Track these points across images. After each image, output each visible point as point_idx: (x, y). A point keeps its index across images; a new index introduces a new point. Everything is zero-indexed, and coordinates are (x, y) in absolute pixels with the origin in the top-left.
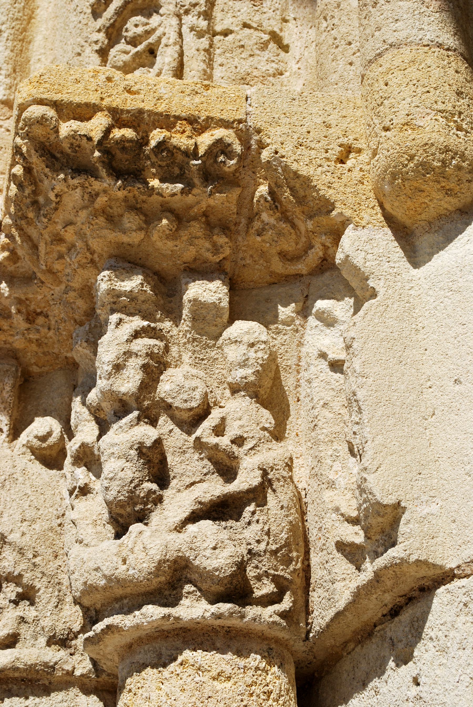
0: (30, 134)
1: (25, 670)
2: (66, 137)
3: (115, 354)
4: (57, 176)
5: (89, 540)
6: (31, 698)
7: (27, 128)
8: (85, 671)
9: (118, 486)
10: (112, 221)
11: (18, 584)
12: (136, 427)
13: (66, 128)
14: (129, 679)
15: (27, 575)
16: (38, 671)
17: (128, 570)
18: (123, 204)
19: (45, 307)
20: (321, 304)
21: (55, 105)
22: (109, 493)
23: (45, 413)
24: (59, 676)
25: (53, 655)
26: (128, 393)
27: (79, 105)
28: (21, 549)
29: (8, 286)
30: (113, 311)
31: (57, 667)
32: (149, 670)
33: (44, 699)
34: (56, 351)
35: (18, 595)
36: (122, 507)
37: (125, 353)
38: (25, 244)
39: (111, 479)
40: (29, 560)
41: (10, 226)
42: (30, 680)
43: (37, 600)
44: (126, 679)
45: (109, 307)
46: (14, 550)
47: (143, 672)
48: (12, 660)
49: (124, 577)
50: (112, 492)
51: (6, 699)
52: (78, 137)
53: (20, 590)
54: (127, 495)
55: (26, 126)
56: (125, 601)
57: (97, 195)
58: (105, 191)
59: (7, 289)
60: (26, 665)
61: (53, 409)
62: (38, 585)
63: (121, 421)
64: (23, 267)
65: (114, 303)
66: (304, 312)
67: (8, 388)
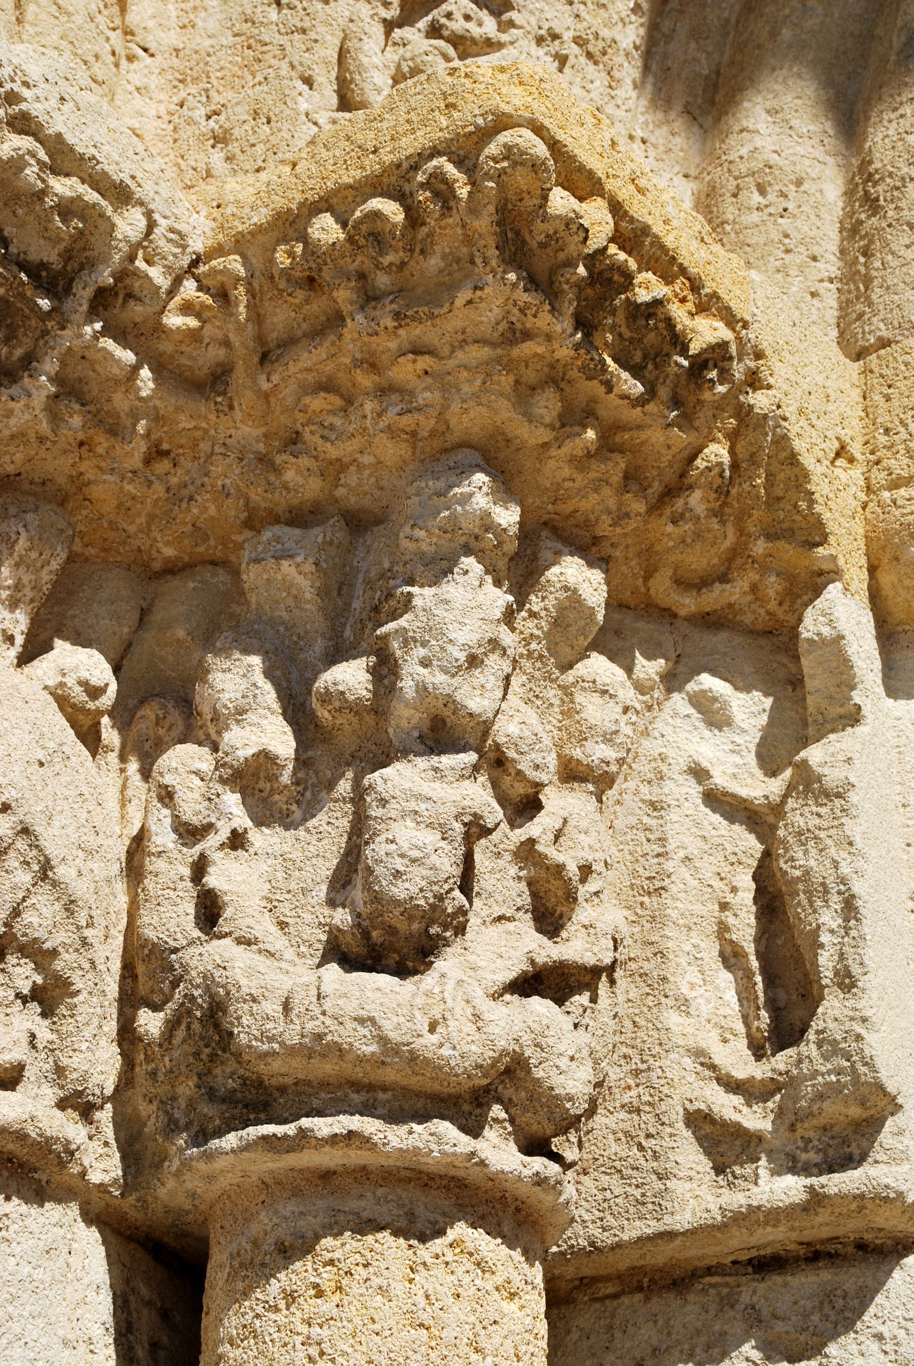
0: (503, 177)
1: (35, 1143)
2: (559, 217)
3: (478, 636)
4: (505, 272)
5: (278, 947)
6: (15, 1200)
7: (505, 164)
8: (107, 1179)
9: (423, 878)
10: (524, 394)
11: (38, 968)
12: (467, 782)
13: (561, 201)
14: (330, 1239)
15: (66, 956)
16: (51, 1152)
17: (441, 1045)
18: (546, 370)
19: (182, 447)
20: (707, 681)
21: (554, 145)
22: (399, 882)
23: (81, 640)
24: (72, 1175)
25: (68, 1128)
26: (480, 715)
27: (581, 168)
28: (72, 902)
29: (155, 380)
30: (468, 551)
31: (77, 1155)
32: (385, 1236)
33: (34, 1210)
34: (132, 529)
35: (35, 988)
36: (411, 918)
37: (490, 641)
38: (250, 326)
39: (413, 861)
40: (79, 928)
41: (238, 279)
42: (21, 1165)
44: (317, 1238)
45: (464, 538)
47: (370, 1238)
48: (24, 1117)
49: (430, 1055)
50: (407, 885)
52: (574, 227)
53: (39, 980)
54: (432, 900)
55: (506, 158)
56: (381, 1096)
57: (527, 335)
58: (549, 338)
59: (151, 385)
60: (41, 1135)
61: (94, 636)
62: (79, 984)
63: (436, 758)
64: (190, 357)
65: (476, 538)
66: (672, 681)
67: (55, 565)
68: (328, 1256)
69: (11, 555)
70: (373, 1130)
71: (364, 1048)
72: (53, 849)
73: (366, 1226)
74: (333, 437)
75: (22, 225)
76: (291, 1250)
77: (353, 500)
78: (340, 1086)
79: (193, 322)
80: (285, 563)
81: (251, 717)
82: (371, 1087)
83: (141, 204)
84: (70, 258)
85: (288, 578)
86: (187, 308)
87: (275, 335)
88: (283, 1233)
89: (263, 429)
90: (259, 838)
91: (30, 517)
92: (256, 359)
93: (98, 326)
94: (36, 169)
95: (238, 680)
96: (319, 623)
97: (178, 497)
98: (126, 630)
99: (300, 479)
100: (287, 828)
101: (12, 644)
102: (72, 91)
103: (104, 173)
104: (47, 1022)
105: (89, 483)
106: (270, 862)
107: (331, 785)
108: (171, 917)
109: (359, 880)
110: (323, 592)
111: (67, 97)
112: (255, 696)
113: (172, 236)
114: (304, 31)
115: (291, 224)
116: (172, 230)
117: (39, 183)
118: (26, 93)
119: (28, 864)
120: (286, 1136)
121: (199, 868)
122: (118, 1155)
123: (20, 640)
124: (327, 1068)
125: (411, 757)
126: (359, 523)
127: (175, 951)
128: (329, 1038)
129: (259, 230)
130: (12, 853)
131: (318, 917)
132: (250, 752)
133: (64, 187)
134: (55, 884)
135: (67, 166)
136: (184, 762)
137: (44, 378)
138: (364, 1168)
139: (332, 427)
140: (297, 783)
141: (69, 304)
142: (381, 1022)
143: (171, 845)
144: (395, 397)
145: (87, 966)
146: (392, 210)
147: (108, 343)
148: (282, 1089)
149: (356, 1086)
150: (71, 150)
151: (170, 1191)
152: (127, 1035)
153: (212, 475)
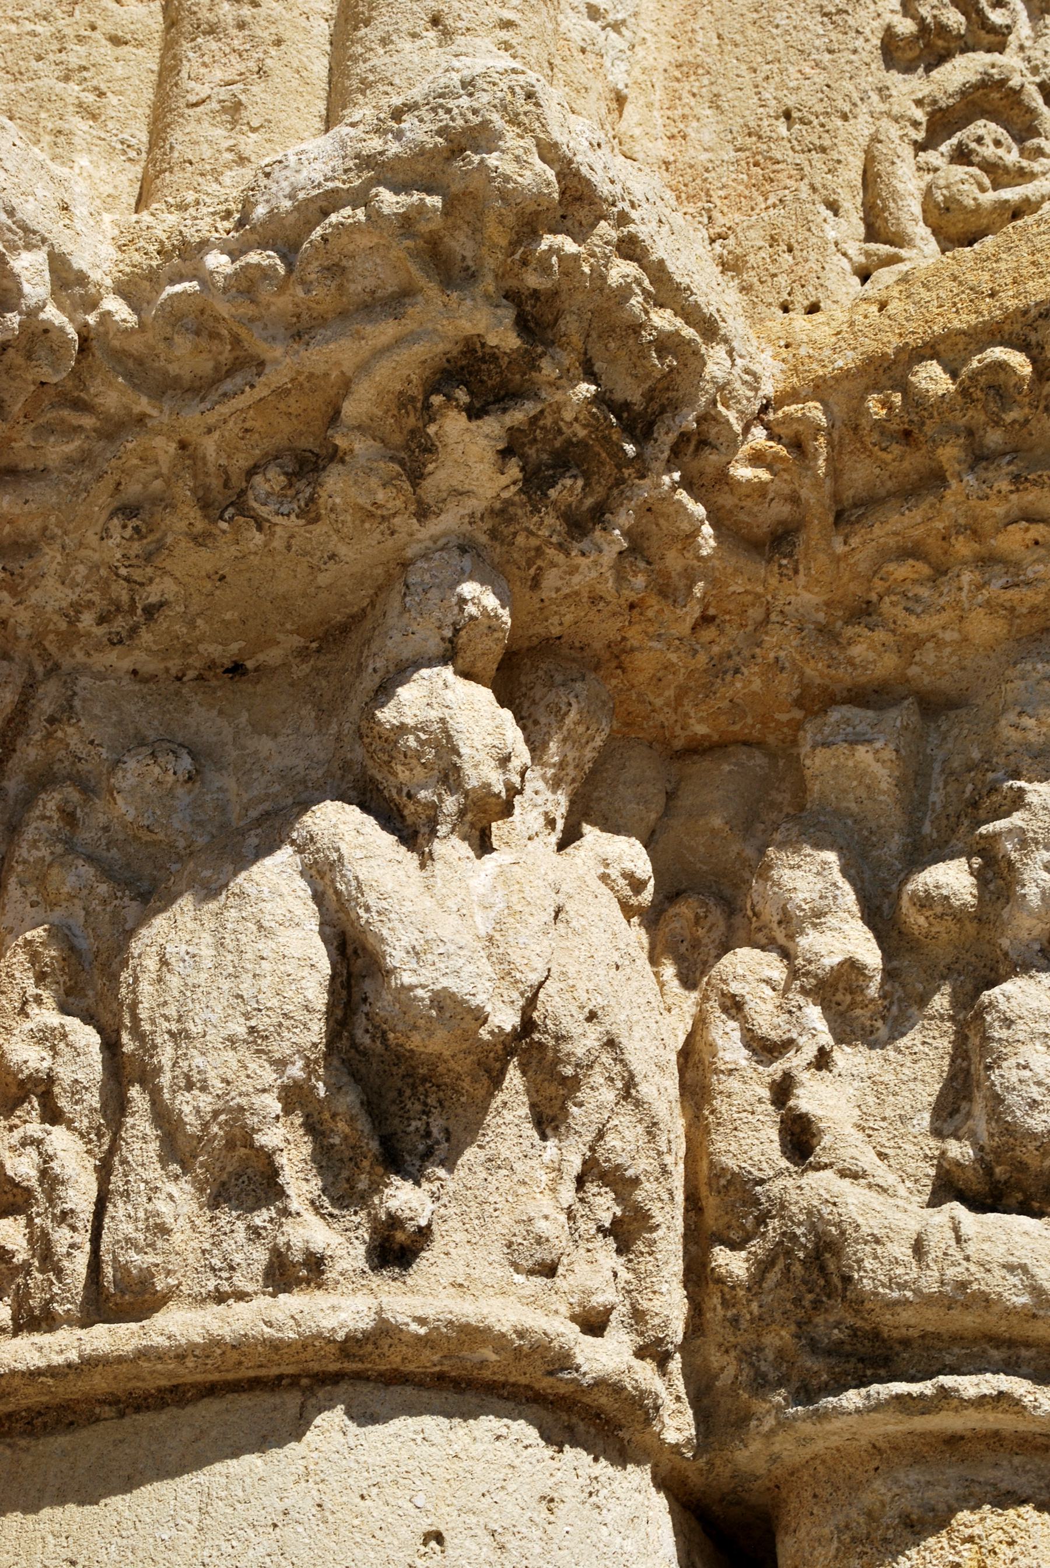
6: (603, 1462)
11: (619, 1199)
14: (966, 1512)
16: (642, 1406)
19: (729, 613)
23: (612, 826)
28: (655, 1124)
29: (716, 538)
32: (1027, 1510)
34: (659, 702)
35: (616, 1221)
40: (660, 1154)
41: (819, 429)
43: (640, 1246)
44: (952, 1512)
46: (640, 1121)
47: (1011, 1513)
50: (1044, 1116)
51: (567, 1447)
56: (1025, 1353)
59: (712, 543)
60: (635, 1388)
61: (621, 822)
67: (598, 742)
68: (968, 1532)
69: (560, 728)
70: (1022, 1391)
71: (1014, 1299)
72: (638, 1066)
73: (1006, 1499)
74: (919, 610)
75: (612, 361)
76: (924, 1523)
77: (927, 680)
78: (975, 1341)
79: (764, 475)
80: (861, 749)
81: (831, 920)
82: (1011, 1343)
83: (726, 340)
84: (652, 399)
85: (863, 765)
86: (757, 459)
87: (851, 493)
88: (906, 1503)
89: (825, 597)
90: (844, 1057)
91: (578, 686)
92: (831, 519)
93: (676, 476)
94: (640, 299)
95: (810, 877)
96: (896, 817)
97: (722, 668)
98: (653, 816)
99: (869, 654)
100: (872, 1046)
101: (553, 829)
103: (697, 305)
104: (622, 1260)
105: (632, 650)
106: (856, 1084)
107: (923, 1000)
108: (752, 1143)
109: (979, 1108)
110: (900, 783)
112: (835, 897)
113: (747, 377)
114: (823, 150)
115: (889, 371)
116: (747, 371)
119: (612, 1080)
120: (922, 1396)
121: (783, 1090)
122: (690, 1412)
123: (560, 824)
124: (968, 1321)
125: (1033, 972)
126: (934, 706)
127: (761, 1182)
128: (975, 1286)
129: (846, 374)
130: (597, 1068)
131: (918, 1148)
132: (836, 960)
133: (663, 320)
134: (638, 1103)
136: (749, 969)
137: (617, 532)
138: (996, 1433)
139: (917, 599)
140: (883, 997)
141: (649, 450)
142: (1035, 1271)
143: (744, 1063)
144: (998, 569)
145: (665, 1196)
146: (1019, 362)
147: (682, 495)
148: (906, 1343)
149: (995, 1341)
150: (671, 279)
151: (749, 1455)
152: (697, 1275)
153: (766, 645)
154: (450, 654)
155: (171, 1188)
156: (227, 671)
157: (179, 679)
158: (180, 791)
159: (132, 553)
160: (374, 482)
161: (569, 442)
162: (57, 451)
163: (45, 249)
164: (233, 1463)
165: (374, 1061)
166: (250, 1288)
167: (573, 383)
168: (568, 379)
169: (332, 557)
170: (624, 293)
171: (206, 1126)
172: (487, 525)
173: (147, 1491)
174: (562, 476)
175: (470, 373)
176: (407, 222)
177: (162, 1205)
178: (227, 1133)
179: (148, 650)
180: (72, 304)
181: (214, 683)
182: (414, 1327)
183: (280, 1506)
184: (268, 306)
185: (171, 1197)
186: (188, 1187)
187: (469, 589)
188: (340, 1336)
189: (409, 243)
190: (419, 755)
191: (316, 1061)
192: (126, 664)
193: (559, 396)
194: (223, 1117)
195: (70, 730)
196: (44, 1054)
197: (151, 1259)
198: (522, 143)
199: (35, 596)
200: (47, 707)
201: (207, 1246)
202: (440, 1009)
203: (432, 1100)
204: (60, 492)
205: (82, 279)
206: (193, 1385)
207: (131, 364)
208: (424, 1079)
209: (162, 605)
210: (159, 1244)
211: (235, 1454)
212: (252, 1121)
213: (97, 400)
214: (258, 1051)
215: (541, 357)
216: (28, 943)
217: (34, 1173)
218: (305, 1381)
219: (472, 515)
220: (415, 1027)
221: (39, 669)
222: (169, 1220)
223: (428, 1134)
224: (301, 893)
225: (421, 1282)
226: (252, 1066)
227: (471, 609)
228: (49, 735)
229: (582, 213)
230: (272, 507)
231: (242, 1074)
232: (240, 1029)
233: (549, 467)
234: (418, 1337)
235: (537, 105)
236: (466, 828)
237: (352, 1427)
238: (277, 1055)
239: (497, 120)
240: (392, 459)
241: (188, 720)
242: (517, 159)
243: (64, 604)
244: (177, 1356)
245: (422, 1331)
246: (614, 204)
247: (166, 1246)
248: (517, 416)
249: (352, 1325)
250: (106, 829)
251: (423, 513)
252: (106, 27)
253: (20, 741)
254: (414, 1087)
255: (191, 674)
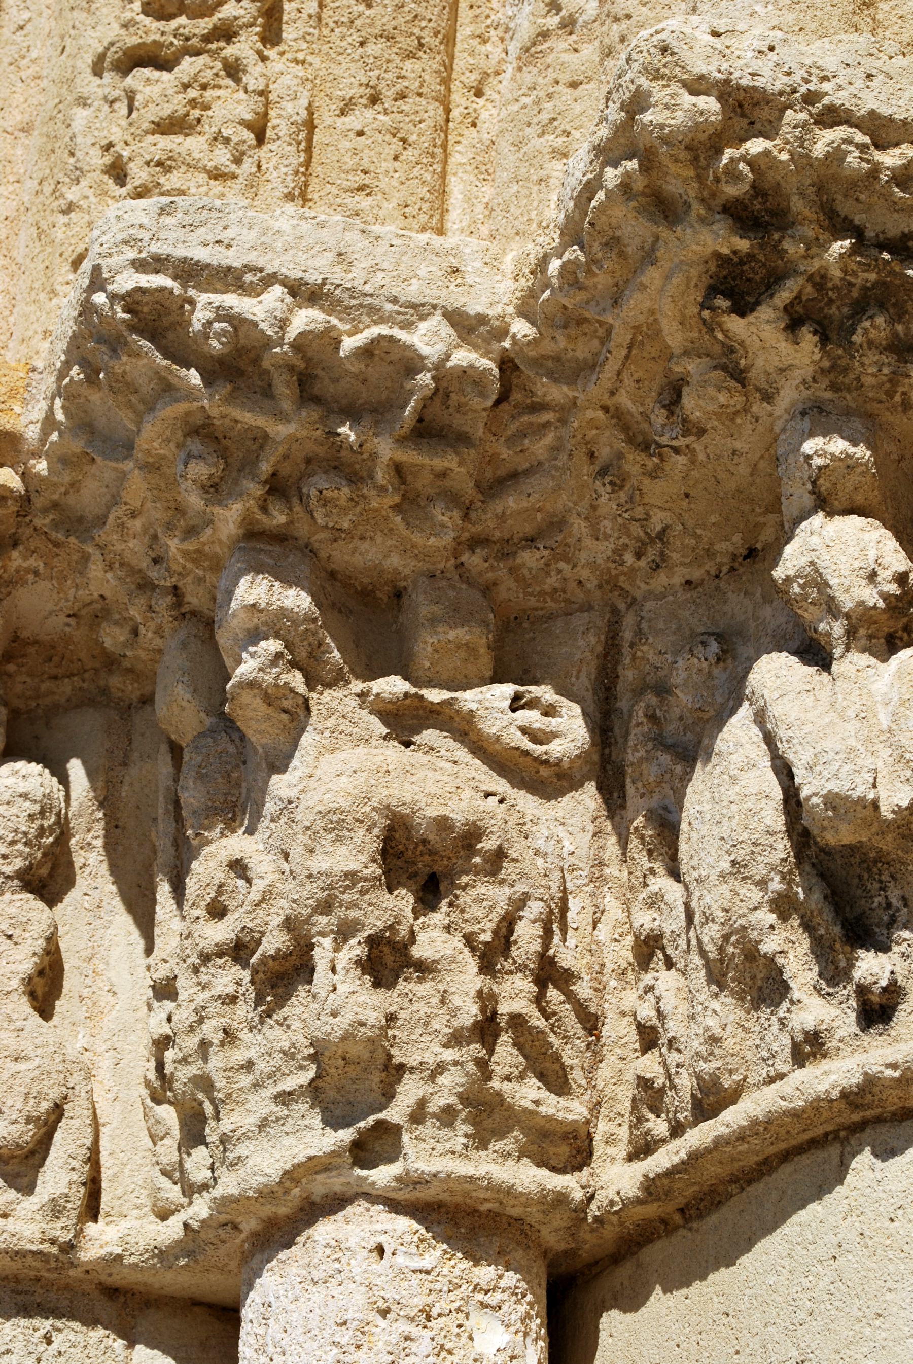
75: (869, 208)
94: (857, 154)
102: (879, 64)
111: (874, 72)
117: (865, 165)
118: (826, 87)
133: (891, 159)
135: (893, 137)
150: (891, 119)
154: (825, 503)
155: (715, 1005)
156: (745, 558)
157: (717, 576)
158: (716, 671)
159: (623, 501)
160: (711, 391)
161: (864, 289)
162: (540, 447)
163: (439, 312)
164: (802, 1213)
165: (837, 857)
166: (784, 1068)
167: (825, 247)
168: (817, 245)
169: (734, 452)
170: (836, 156)
171: (721, 949)
172: (825, 382)
173: (759, 1247)
174: (860, 321)
175: (734, 279)
176: (625, 187)
177: (711, 1022)
178: (742, 950)
179: (683, 564)
180: (484, 340)
181: (741, 570)
182: (889, 1073)
183: (835, 1240)
184: (595, 287)
185: (715, 1012)
186: (729, 1000)
187: (809, 447)
188: (835, 1094)
189: (633, 204)
190: (805, 597)
191: (790, 872)
192: (677, 580)
193: (816, 264)
194: (733, 938)
195: (645, 648)
196: (655, 915)
197: (715, 1064)
198: (668, 91)
199: (583, 557)
200: (628, 635)
201: (758, 1042)
202: (834, 808)
203: (885, 877)
204: (553, 477)
205: (482, 319)
206: (776, 1155)
207: (550, 364)
208: (875, 862)
209: (664, 530)
210: (716, 1051)
211: (803, 1207)
212: (754, 935)
213: (548, 398)
214: (743, 878)
215: (780, 241)
216: (636, 829)
217: (653, 1013)
218: (842, 1134)
219: (804, 382)
220: (824, 829)
221: (622, 606)
222: (717, 1031)
223: (889, 905)
224: (755, 739)
225: (903, 1031)
226: (742, 891)
227: (818, 461)
228: (634, 658)
229: (765, 113)
230: (667, 436)
231: (737, 900)
232: (726, 865)
233: (848, 318)
234: (898, 1080)
235: (673, 54)
236: (864, 642)
237: (878, 1163)
238: (758, 877)
239: (644, 82)
240: (715, 368)
241: (726, 608)
242: (667, 107)
243: (609, 554)
244: (738, 1139)
245: (897, 1074)
246: (794, 91)
247: (722, 1052)
248: (784, 296)
249: (845, 1083)
250: (681, 718)
251: (768, 398)
252: (565, 78)
253: (620, 668)
254: (869, 870)
255: (725, 569)
